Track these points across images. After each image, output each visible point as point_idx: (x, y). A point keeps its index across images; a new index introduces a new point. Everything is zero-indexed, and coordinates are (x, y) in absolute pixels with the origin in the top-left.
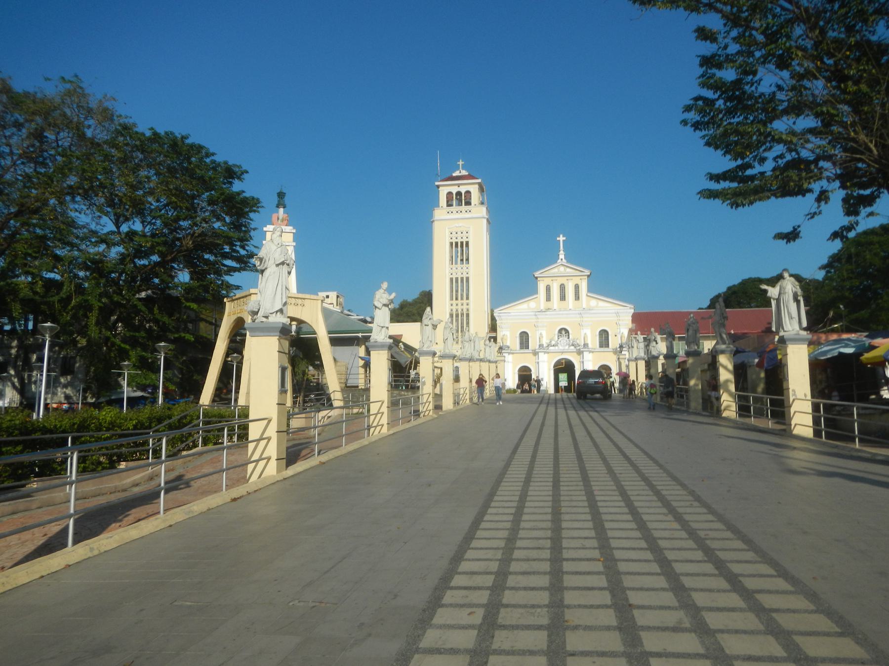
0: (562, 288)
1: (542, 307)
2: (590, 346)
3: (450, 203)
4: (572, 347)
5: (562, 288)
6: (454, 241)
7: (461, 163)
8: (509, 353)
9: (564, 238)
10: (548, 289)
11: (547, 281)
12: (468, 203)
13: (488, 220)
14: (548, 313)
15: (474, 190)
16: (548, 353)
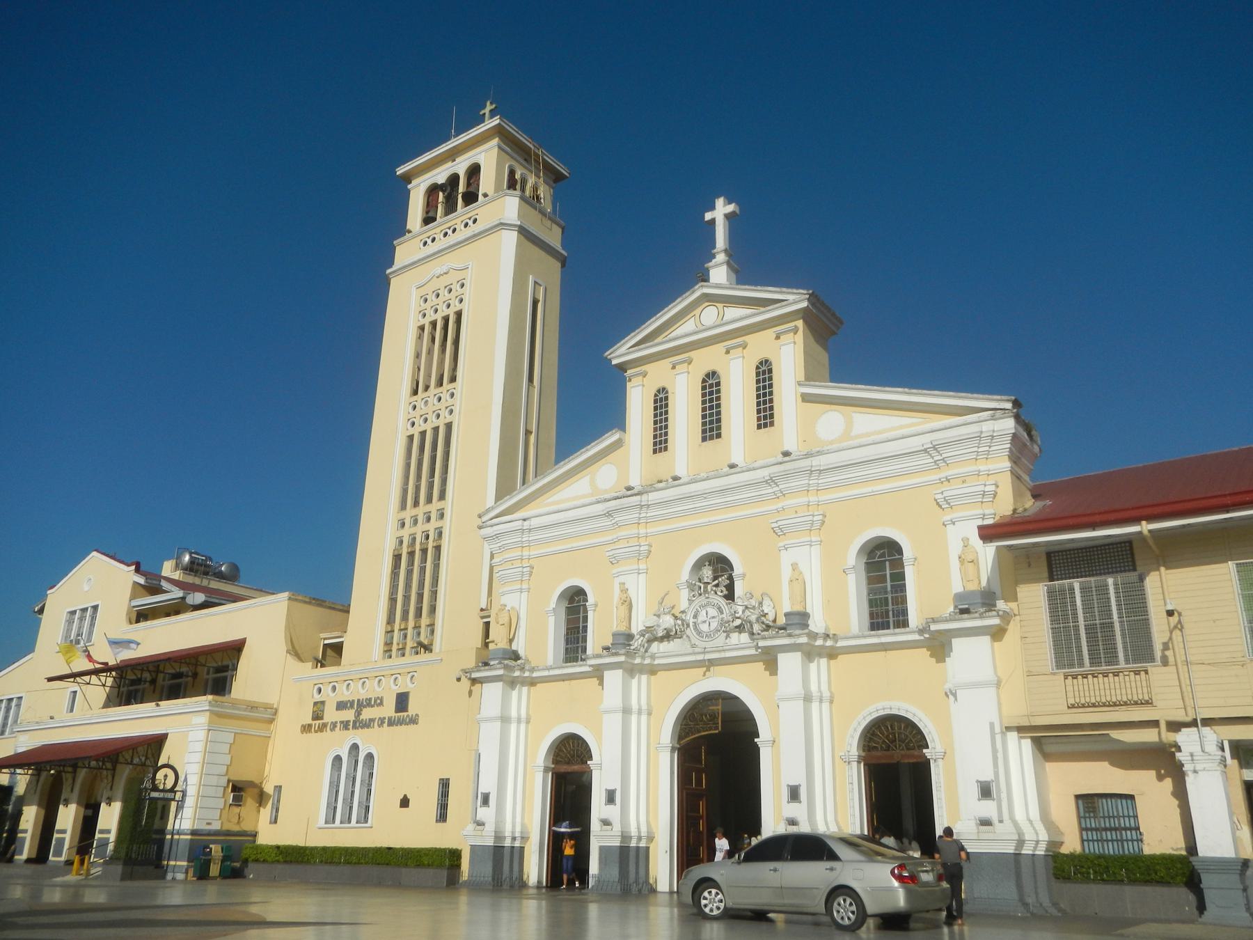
0: (711, 388)
1: (635, 481)
2: (817, 623)
3: (431, 214)
4: (745, 637)
5: (711, 388)
6: (431, 316)
7: (489, 107)
8: (512, 683)
9: (731, 208)
10: (661, 403)
11: (658, 374)
12: (471, 198)
13: (523, 231)
14: (653, 497)
15: (488, 157)
16: (652, 671)
